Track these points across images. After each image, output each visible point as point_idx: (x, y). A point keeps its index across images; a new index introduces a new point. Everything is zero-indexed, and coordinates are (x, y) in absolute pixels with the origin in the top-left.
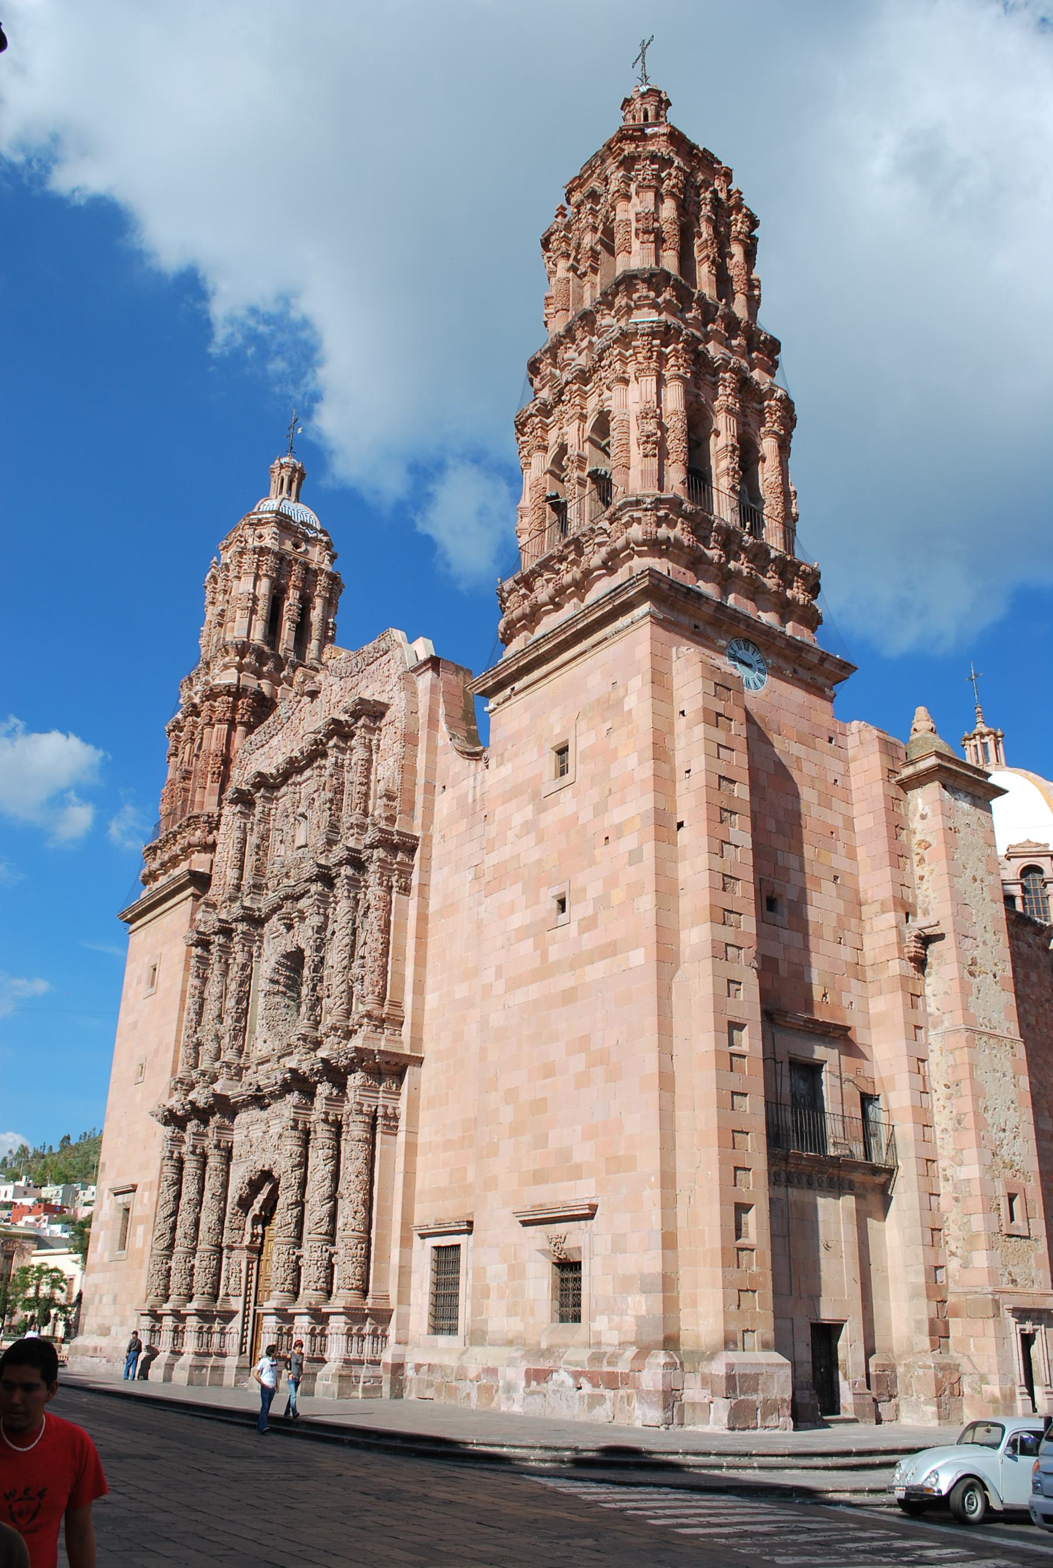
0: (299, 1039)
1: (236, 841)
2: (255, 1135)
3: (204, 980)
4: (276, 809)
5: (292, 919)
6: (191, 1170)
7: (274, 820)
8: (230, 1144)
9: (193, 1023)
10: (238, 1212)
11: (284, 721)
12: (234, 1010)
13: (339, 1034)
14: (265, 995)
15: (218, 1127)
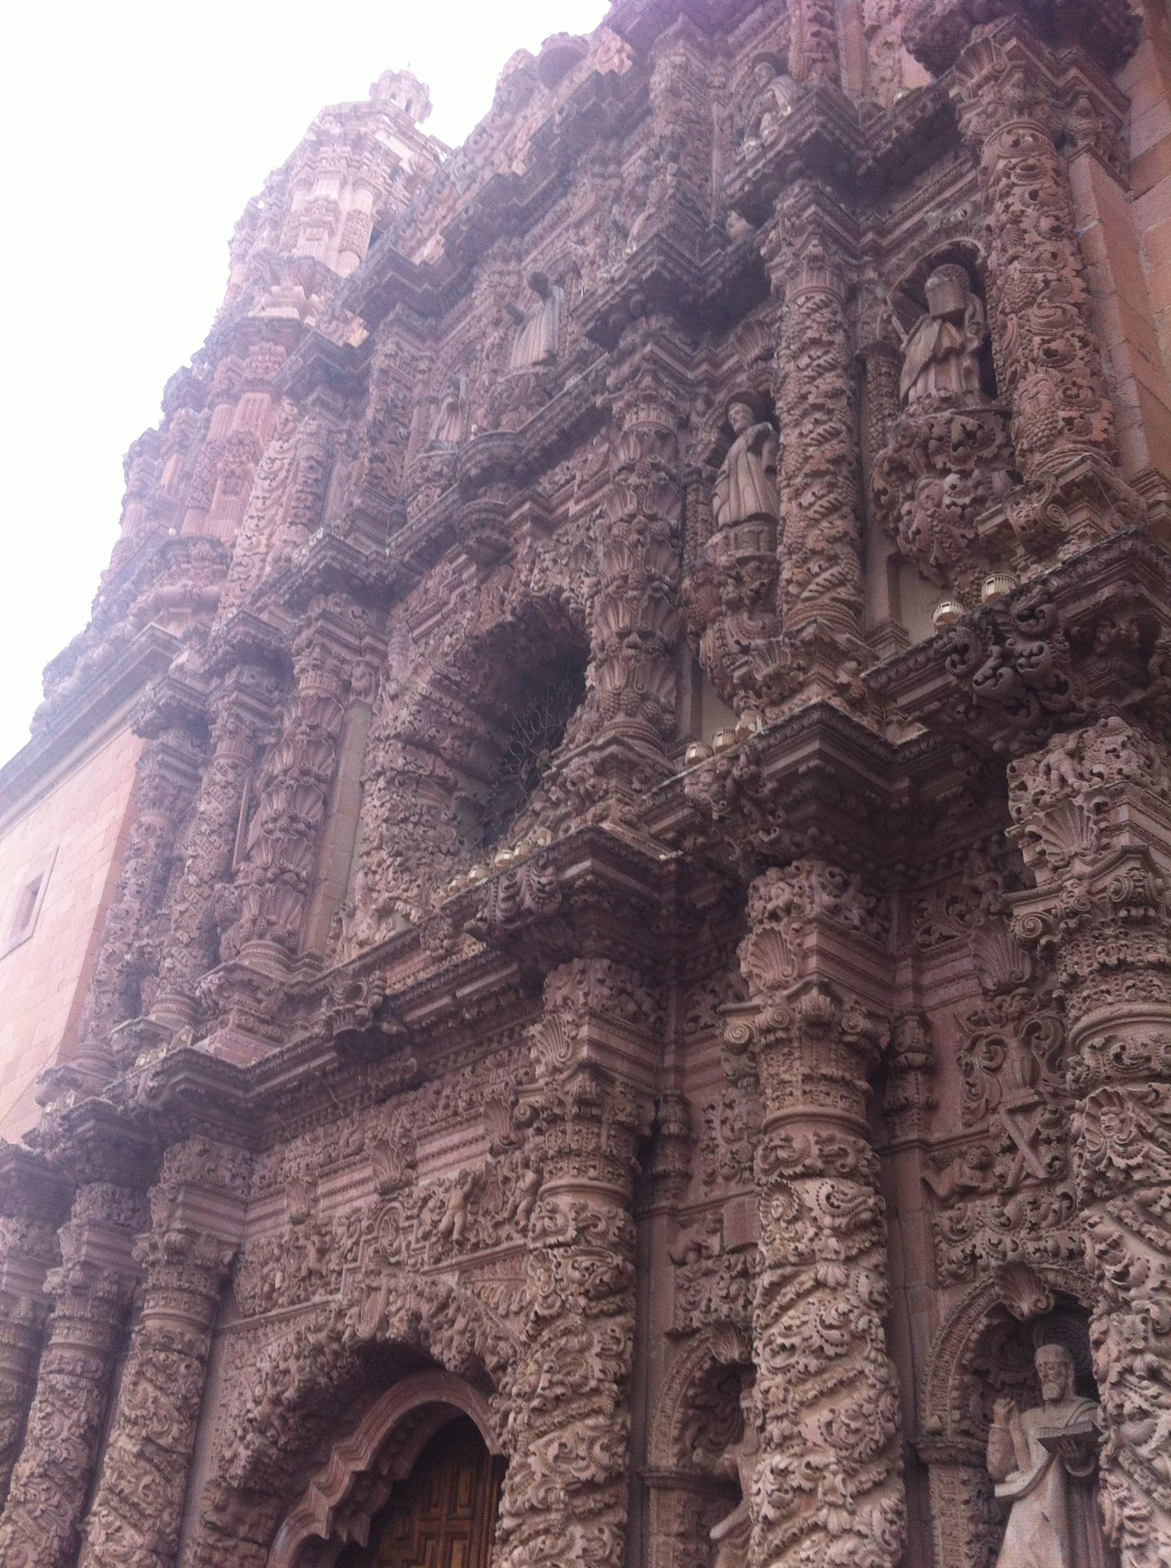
0: (601, 770)
1: (303, 464)
2: (341, 1211)
3: (180, 817)
4: (432, 361)
5: (506, 531)
6: (68, 1354)
7: (426, 383)
8: (228, 1256)
9: (131, 923)
10: (239, 1520)
11: (459, 187)
12: (283, 822)
13: (844, 678)
14: (390, 782)
15: (190, 1186)
